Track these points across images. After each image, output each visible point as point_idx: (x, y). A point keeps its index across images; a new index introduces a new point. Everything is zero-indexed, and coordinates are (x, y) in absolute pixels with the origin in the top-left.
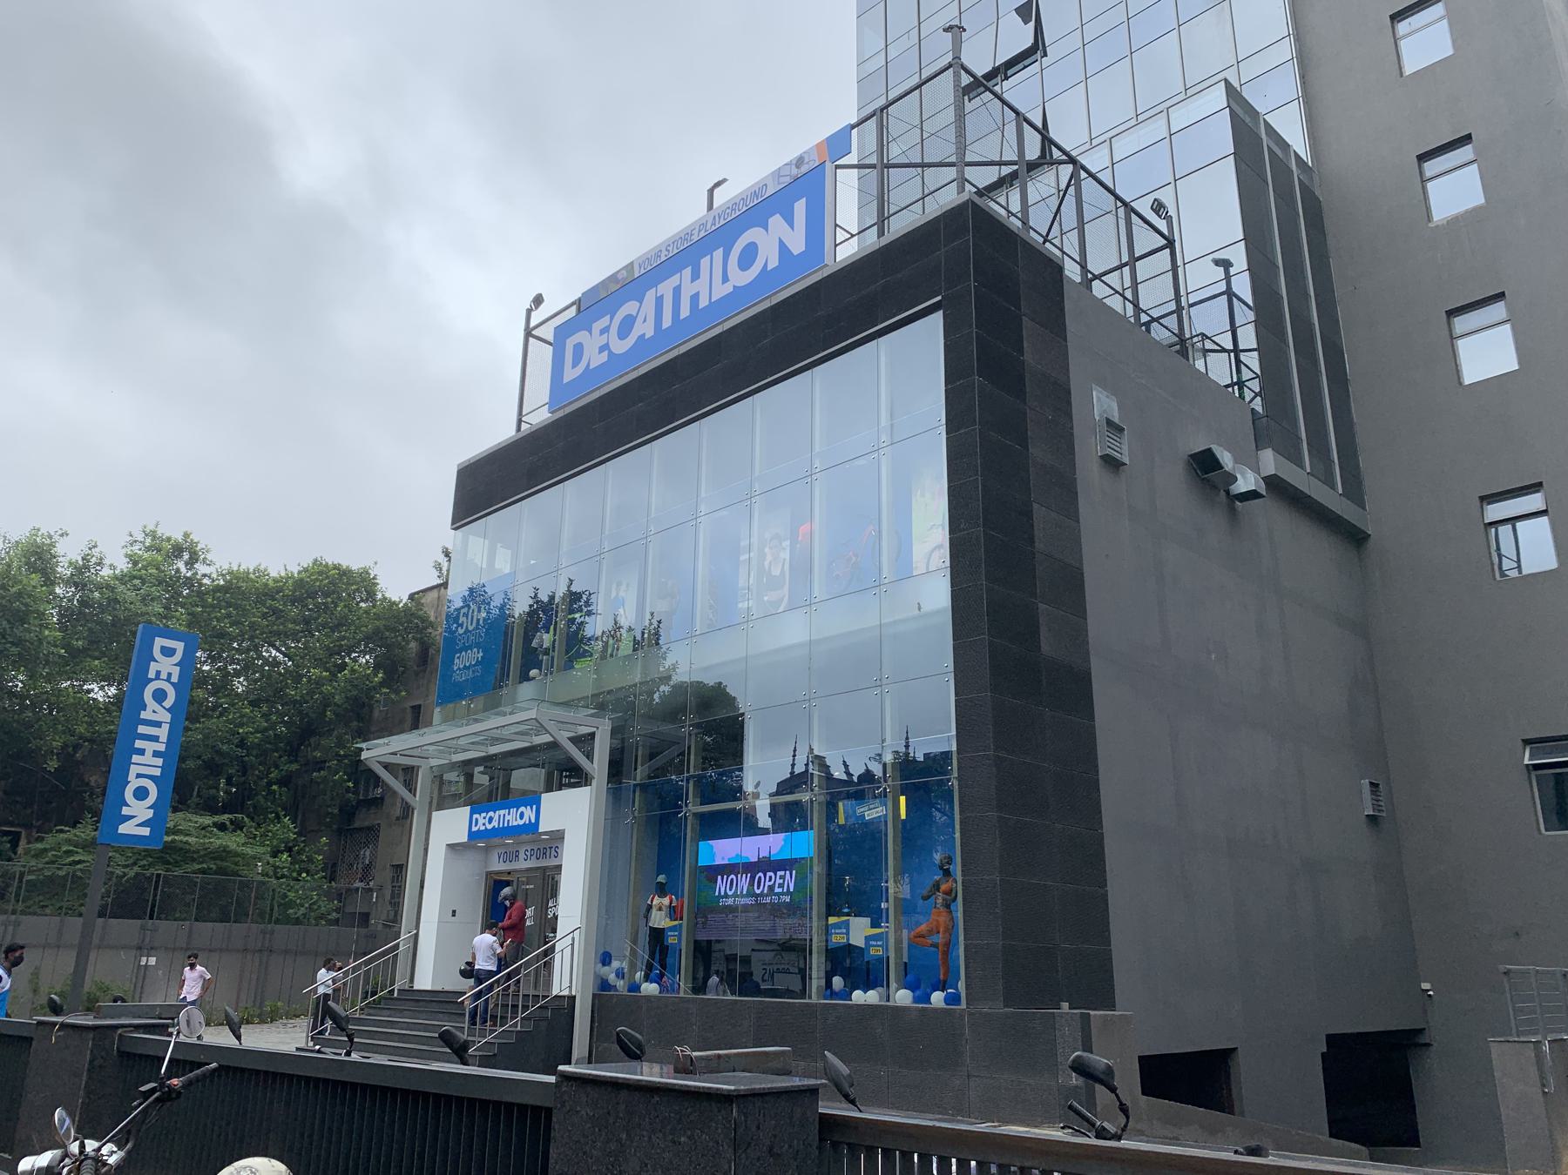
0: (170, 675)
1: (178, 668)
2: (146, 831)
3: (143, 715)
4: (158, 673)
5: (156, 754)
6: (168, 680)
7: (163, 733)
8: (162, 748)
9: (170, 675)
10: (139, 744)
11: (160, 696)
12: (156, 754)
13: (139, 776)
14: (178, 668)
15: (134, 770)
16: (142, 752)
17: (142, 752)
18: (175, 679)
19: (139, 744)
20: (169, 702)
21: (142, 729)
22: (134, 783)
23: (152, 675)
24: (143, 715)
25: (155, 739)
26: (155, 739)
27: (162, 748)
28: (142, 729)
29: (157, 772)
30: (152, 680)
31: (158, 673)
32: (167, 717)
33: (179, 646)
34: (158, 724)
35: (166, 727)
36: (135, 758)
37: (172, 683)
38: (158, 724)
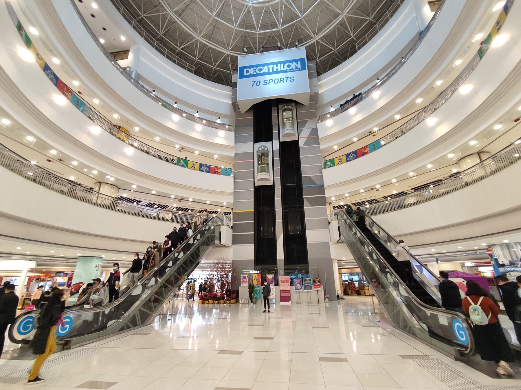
0: (254, 70)
1: (251, 68)
2: (299, 62)
3: (267, 71)
4: (254, 72)
5: (277, 66)
6: (255, 69)
7: (270, 67)
8: (275, 66)
9: (254, 70)
10: (275, 70)
11: (260, 70)
12: (277, 66)
13: (284, 68)
14: (251, 68)
15: (282, 69)
16: (277, 69)
17: (277, 69)
18: (255, 68)
19: (275, 70)
20: (262, 68)
21: (271, 71)
22: (286, 68)
23: (255, 73)
24: (267, 71)
25: (273, 68)
26: (273, 68)
27: (275, 66)
28: (271, 71)
29: (282, 65)
30: (256, 73)
31: (254, 72)
32: (266, 67)
33: (245, 70)
34: (269, 68)
35: (269, 66)
36: (279, 70)
37: (256, 68)
38: (269, 68)
